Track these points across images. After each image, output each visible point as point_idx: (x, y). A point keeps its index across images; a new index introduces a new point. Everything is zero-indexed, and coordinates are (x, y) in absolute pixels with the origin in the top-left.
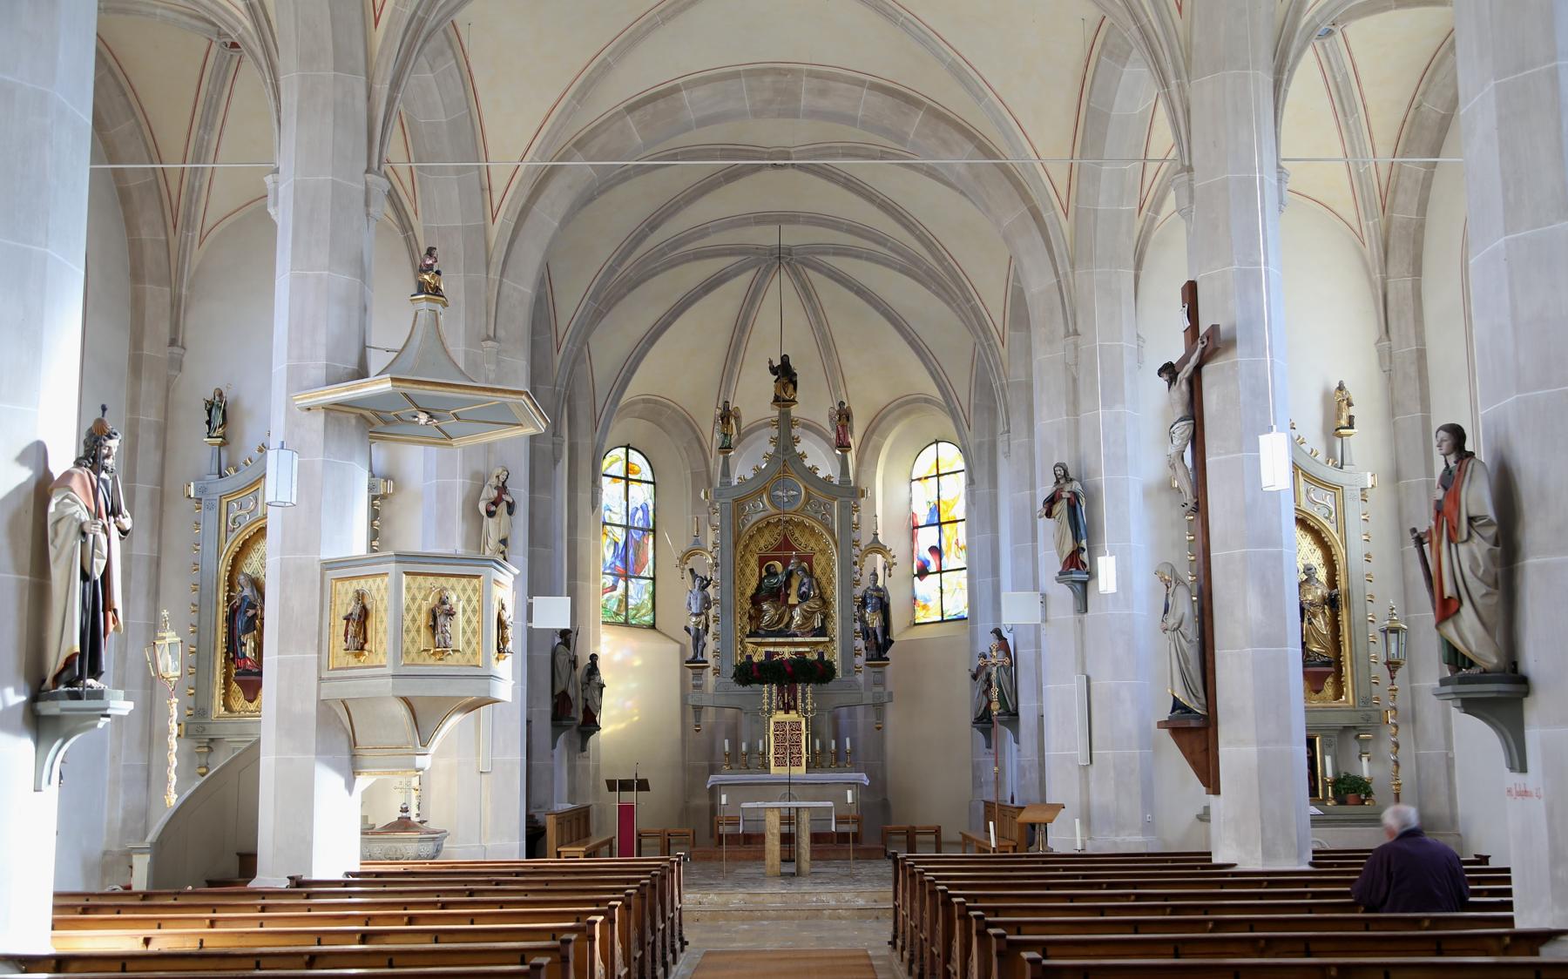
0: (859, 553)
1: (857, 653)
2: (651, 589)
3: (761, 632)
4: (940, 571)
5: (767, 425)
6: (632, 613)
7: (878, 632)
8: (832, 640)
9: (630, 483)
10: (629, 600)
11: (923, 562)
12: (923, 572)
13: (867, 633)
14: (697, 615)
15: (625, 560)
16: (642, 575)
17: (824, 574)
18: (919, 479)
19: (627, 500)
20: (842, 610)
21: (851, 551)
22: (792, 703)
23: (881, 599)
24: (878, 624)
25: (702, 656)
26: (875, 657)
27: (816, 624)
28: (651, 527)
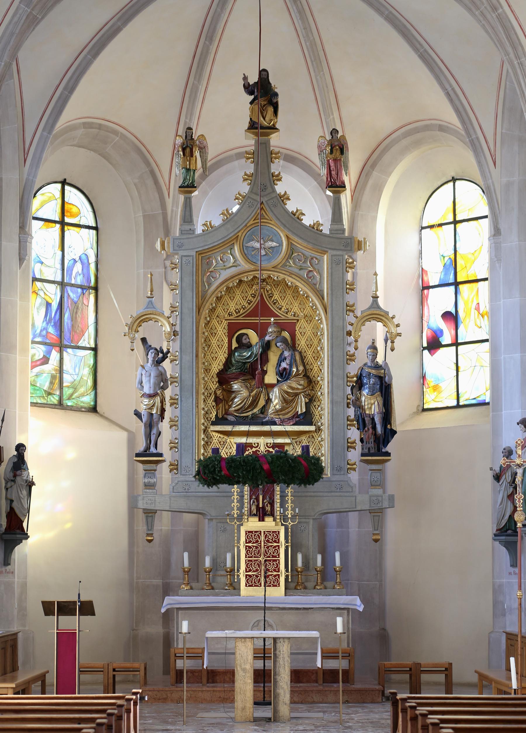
0: (353, 320)
1: (351, 446)
2: (91, 362)
3: (231, 418)
4: (456, 344)
5: (239, 156)
6: (67, 392)
7: (377, 420)
8: (319, 430)
9: (66, 228)
10: (65, 376)
14: (151, 396)
15: (59, 325)
18: (431, 227)
19: (63, 250)
20: (332, 392)
21: (344, 319)
22: (268, 508)
23: (381, 379)
24: (377, 410)
25: (156, 448)
26: (372, 451)
28: (93, 283)
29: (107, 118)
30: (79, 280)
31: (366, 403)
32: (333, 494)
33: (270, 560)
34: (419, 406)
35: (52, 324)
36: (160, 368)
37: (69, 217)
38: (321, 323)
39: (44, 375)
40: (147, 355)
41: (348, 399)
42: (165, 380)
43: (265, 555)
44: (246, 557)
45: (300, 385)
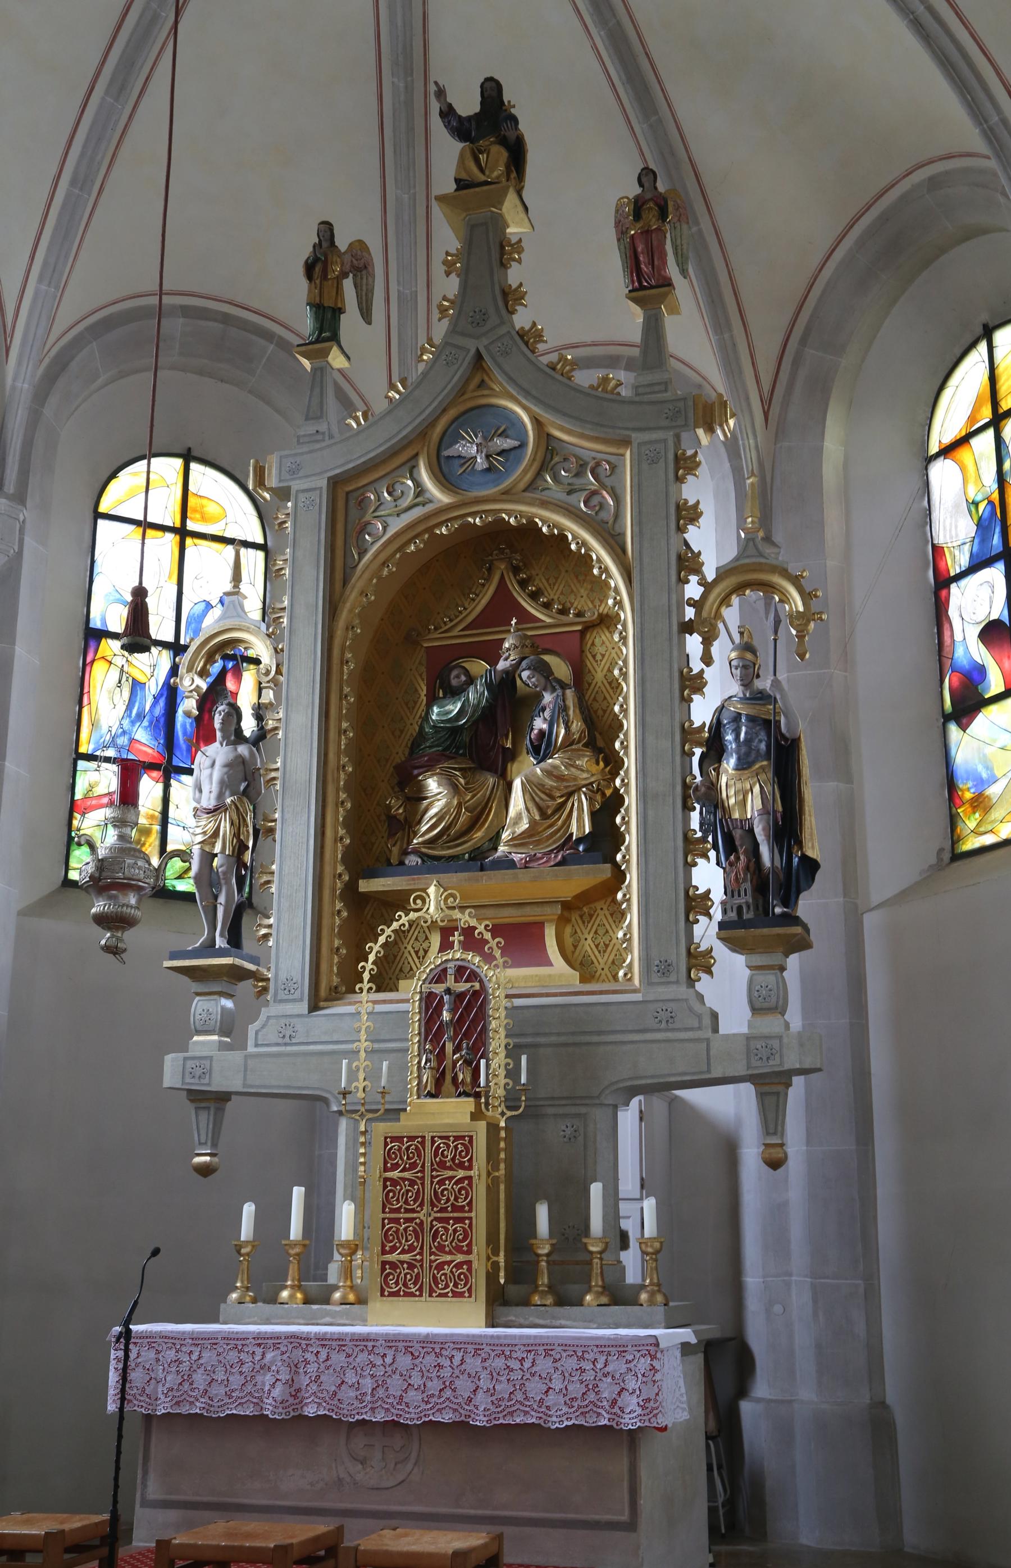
9: (189, 541)
10: (171, 829)
23: (768, 725)
24: (758, 804)
26: (746, 916)
27: (574, 828)
29: (239, 299)
31: (732, 792)
32: (649, 1036)
33: (446, 1220)
34: (941, 850)
35: (145, 723)
37: (198, 520)
43: (433, 1205)
44: (384, 1212)
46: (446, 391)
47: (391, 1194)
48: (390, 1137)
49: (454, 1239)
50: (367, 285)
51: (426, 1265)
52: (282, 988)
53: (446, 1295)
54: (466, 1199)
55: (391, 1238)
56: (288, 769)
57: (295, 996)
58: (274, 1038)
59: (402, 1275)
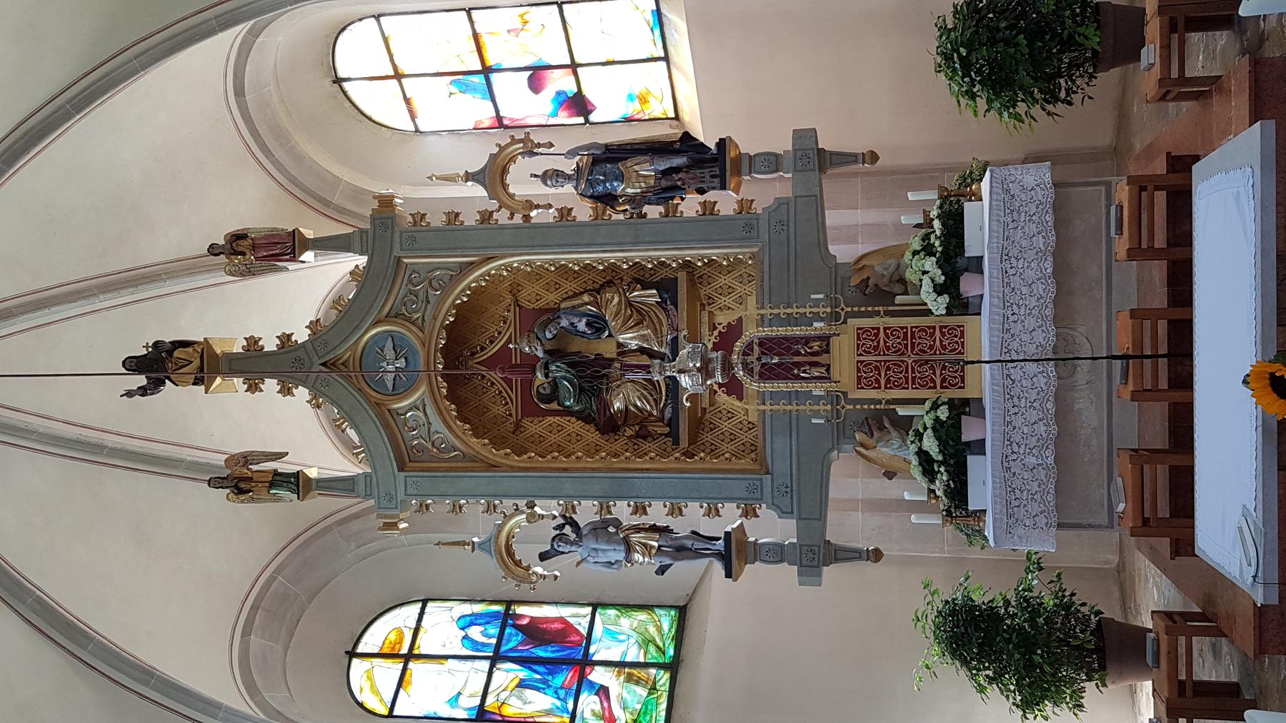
1: (709, 208)
2: (612, 612)
4: (574, 66)
6: (653, 656)
7: (663, 165)
8: (687, 265)
9: (416, 652)
10: (628, 659)
11: (561, 104)
12: (578, 104)
13: (666, 191)
14: (629, 549)
15: (553, 665)
16: (584, 632)
17: (557, 286)
18: (413, 116)
20: (620, 245)
21: (503, 227)
22: (816, 346)
25: (720, 539)
26: (717, 171)
28: (498, 608)
29: (242, 597)
30: (494, 630)
32: (792, 237)
33: (913, 344)
35: (550, 678)
36: (585, 532)
37: (401, 646)
38: (510, 265)
39: (625, 695)
40: (563, 553)
41: (632, 217)
42: (604, 524)
43: (903, 354)
44: (908, 388)
45: (613, 298)
46: (349, 387)
47: (896, 383)
48: (858, 385)
49: (925, 339)
50: (259, 456)
51: (942, 357)
52: (752, 494)
53: (963, 343)
54: (898, 331)
55: (925, 383)
56: (602, 495)
57: (759, 485)
58: (787, 500)
59: (949, 374)
